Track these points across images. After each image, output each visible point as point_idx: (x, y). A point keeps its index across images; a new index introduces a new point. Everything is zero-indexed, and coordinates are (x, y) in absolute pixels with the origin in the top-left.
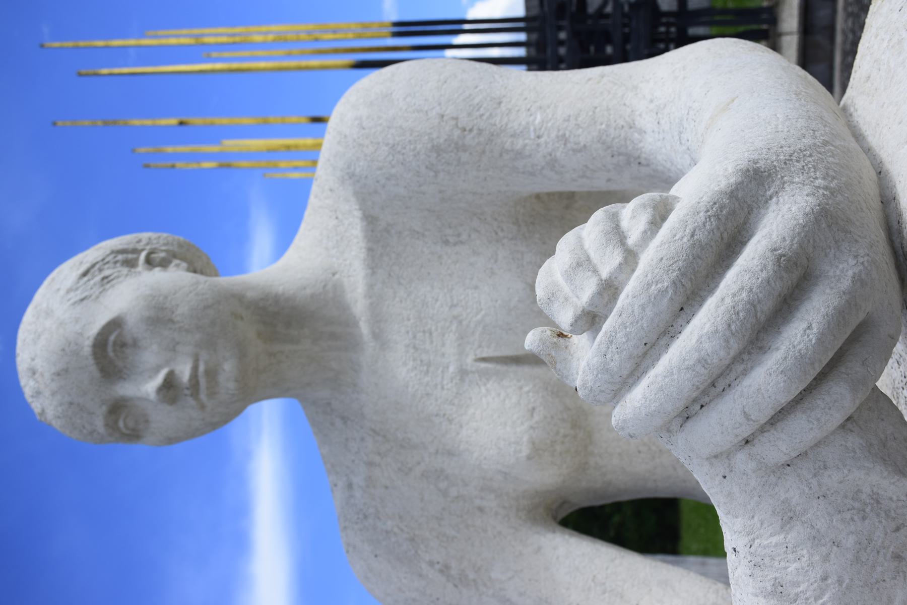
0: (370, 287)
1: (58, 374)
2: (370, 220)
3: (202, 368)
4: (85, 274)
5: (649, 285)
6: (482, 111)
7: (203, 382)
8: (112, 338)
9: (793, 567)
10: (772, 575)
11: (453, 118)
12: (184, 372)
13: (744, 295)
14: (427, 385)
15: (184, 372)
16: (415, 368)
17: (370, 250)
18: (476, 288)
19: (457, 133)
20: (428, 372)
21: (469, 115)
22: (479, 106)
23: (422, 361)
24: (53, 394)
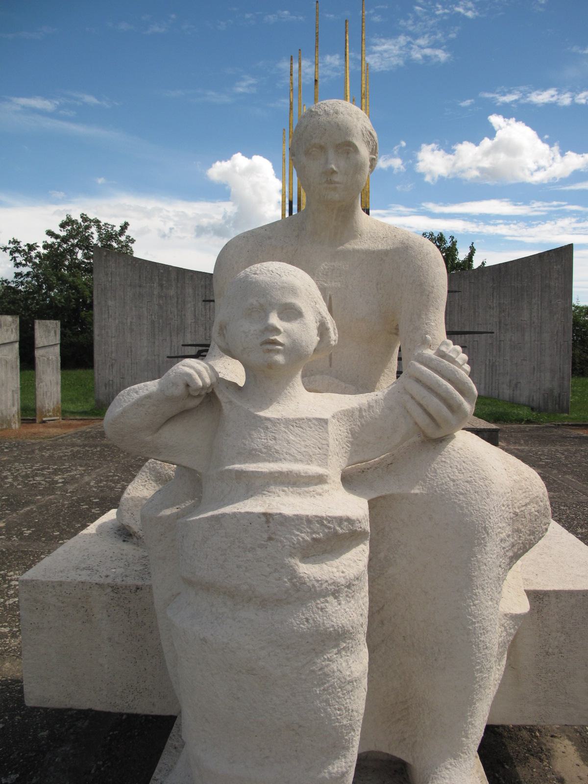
0: (358, 251)
1: (338, 126)
2: (386, 253)
3: (337, 185)
4: (371, 134)
5: (457, 372)
6: (435, 302)
7: (333, 186)
8: (351, 149)
9: (378, 411)
10: (374, 405)
11: (432, 291)
12: (337, 178)
13: (455, 396)
14: (318, 274)
15: (337, 178)
16: (324, 269)
17: (374, 252)
18: (361, 296)
19: (427, 293)
20: (324, 275)
21: (433, 298)
22: (437, 301)
23: (328, 272)
24: (329, 122)
